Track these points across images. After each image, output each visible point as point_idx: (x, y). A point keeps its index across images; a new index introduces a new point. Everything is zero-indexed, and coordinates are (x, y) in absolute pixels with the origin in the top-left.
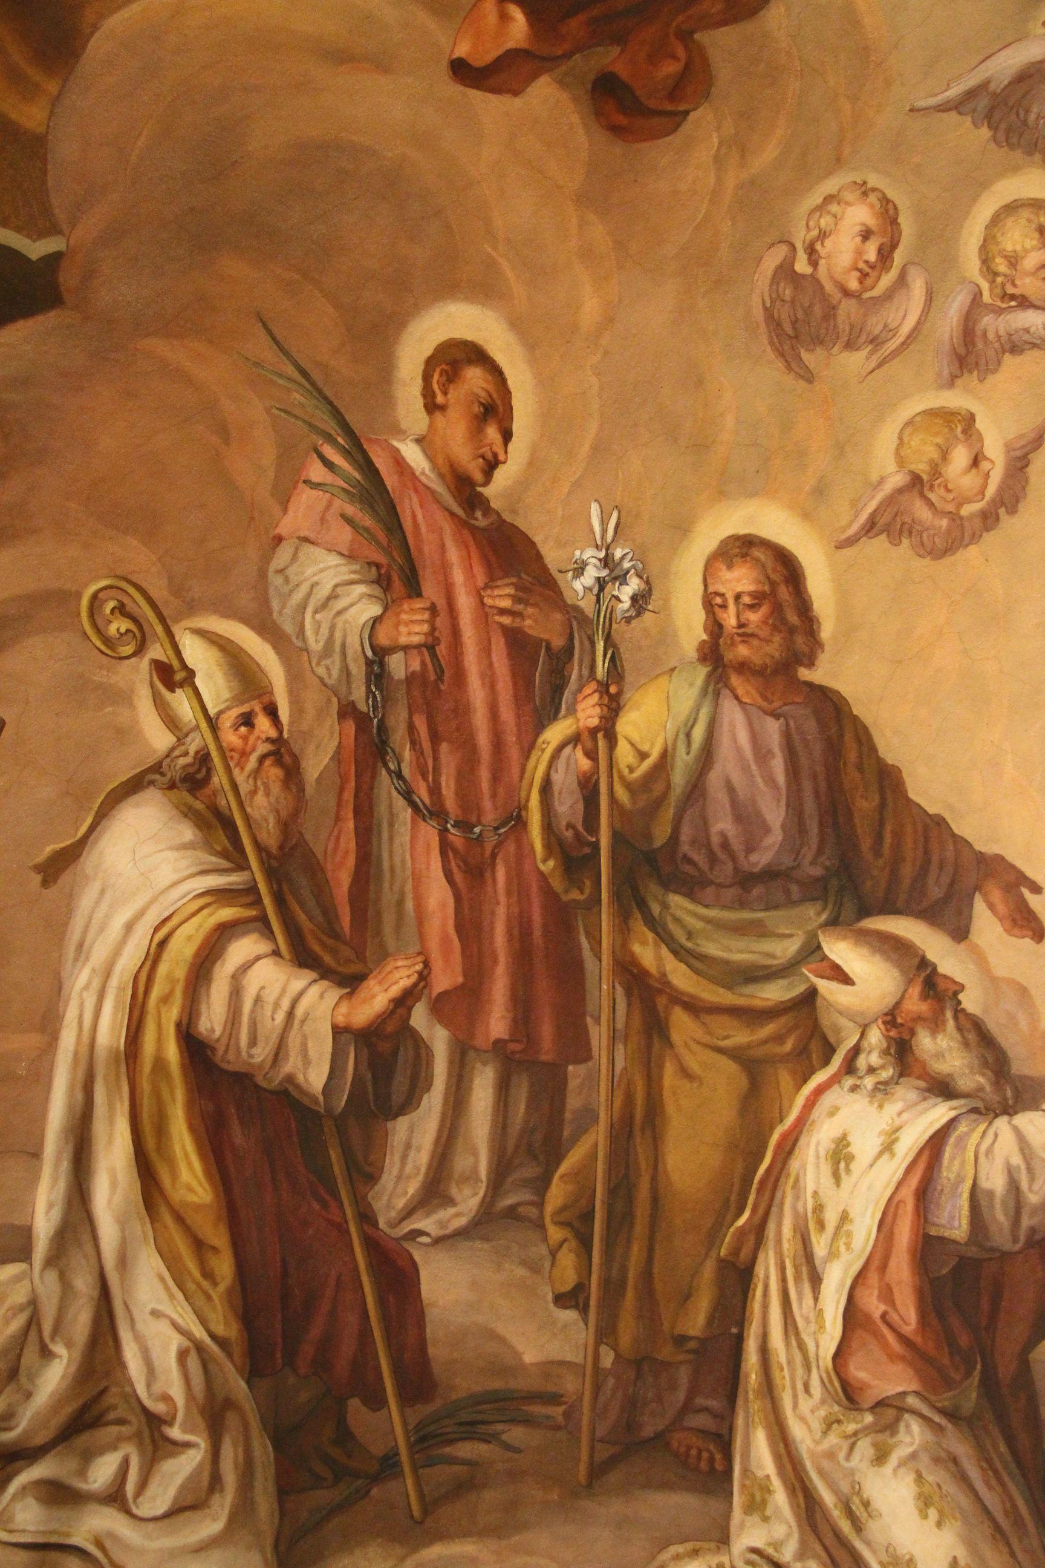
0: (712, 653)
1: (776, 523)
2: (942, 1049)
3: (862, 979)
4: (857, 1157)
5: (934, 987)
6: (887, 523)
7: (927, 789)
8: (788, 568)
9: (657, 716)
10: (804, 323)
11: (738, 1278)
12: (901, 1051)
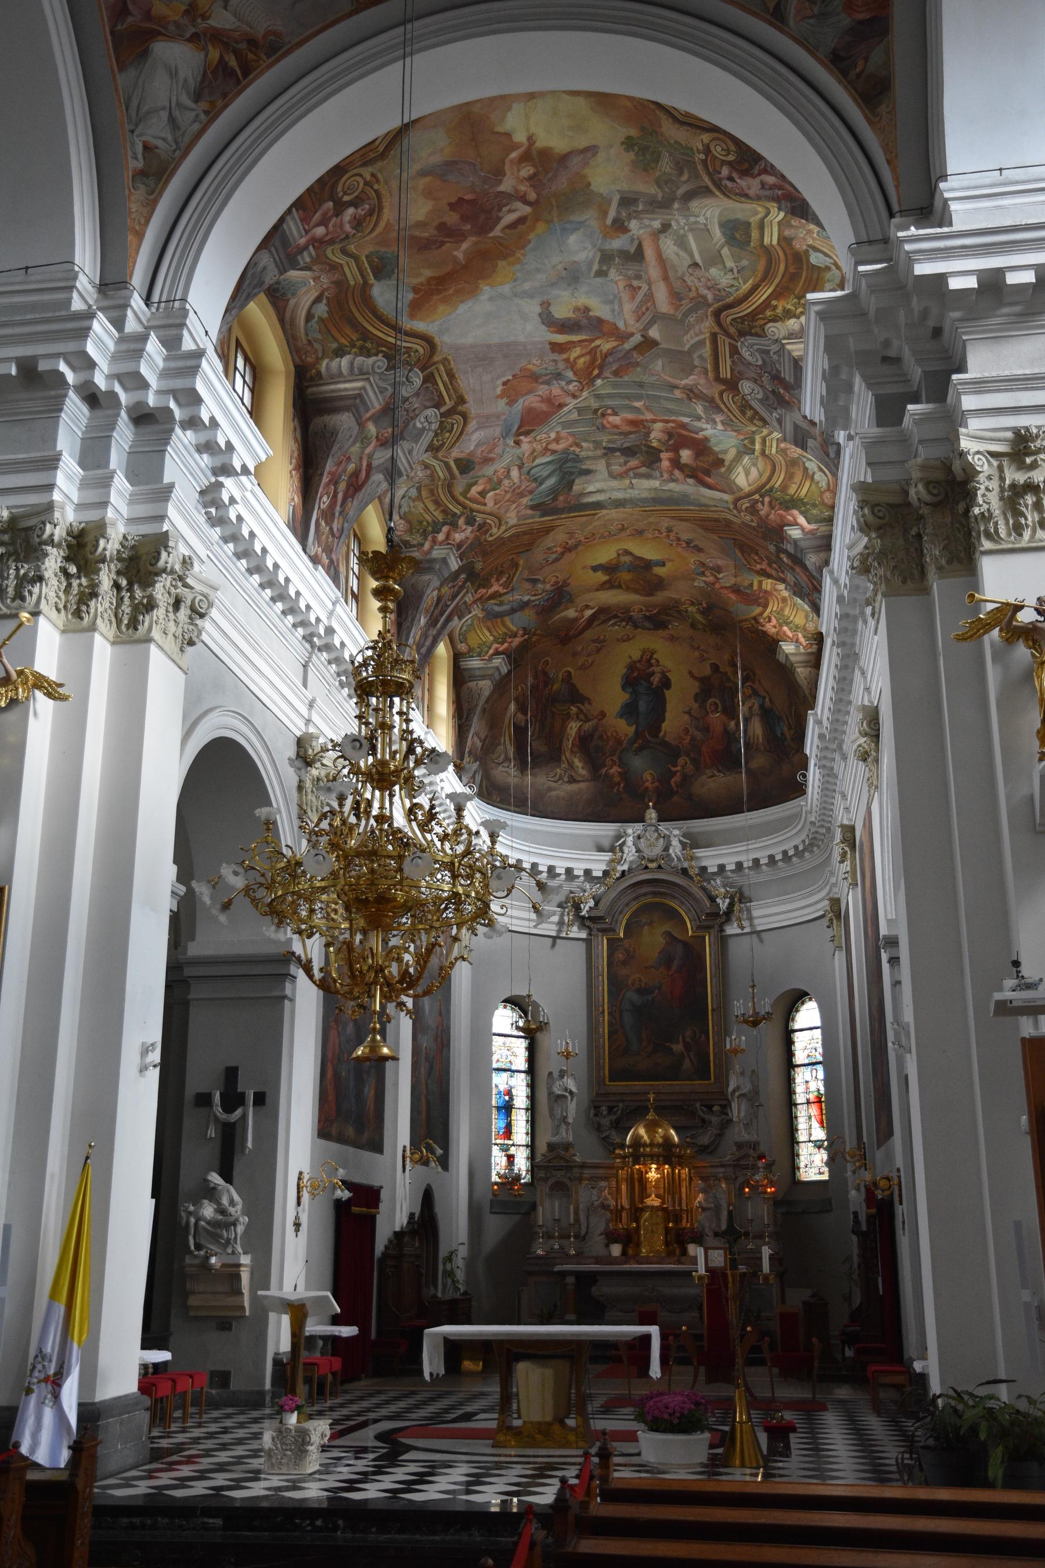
0: (562, 681)
1: (570, 669)
2: (581, 716)
3: (574, 710)
4: (573, 728)
5: (581, 711)
6: (580, 668)
7: (581, 691)
8: (570, 673)
9: (556, 687)
10: (575, 654)
11: (561, 741)
12: (577, 717)
